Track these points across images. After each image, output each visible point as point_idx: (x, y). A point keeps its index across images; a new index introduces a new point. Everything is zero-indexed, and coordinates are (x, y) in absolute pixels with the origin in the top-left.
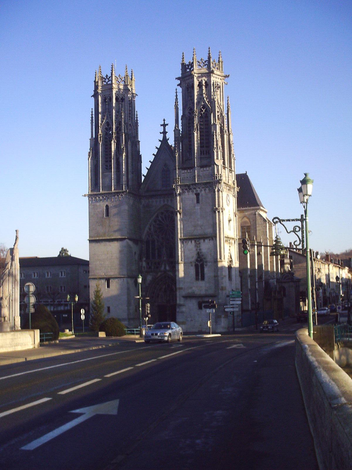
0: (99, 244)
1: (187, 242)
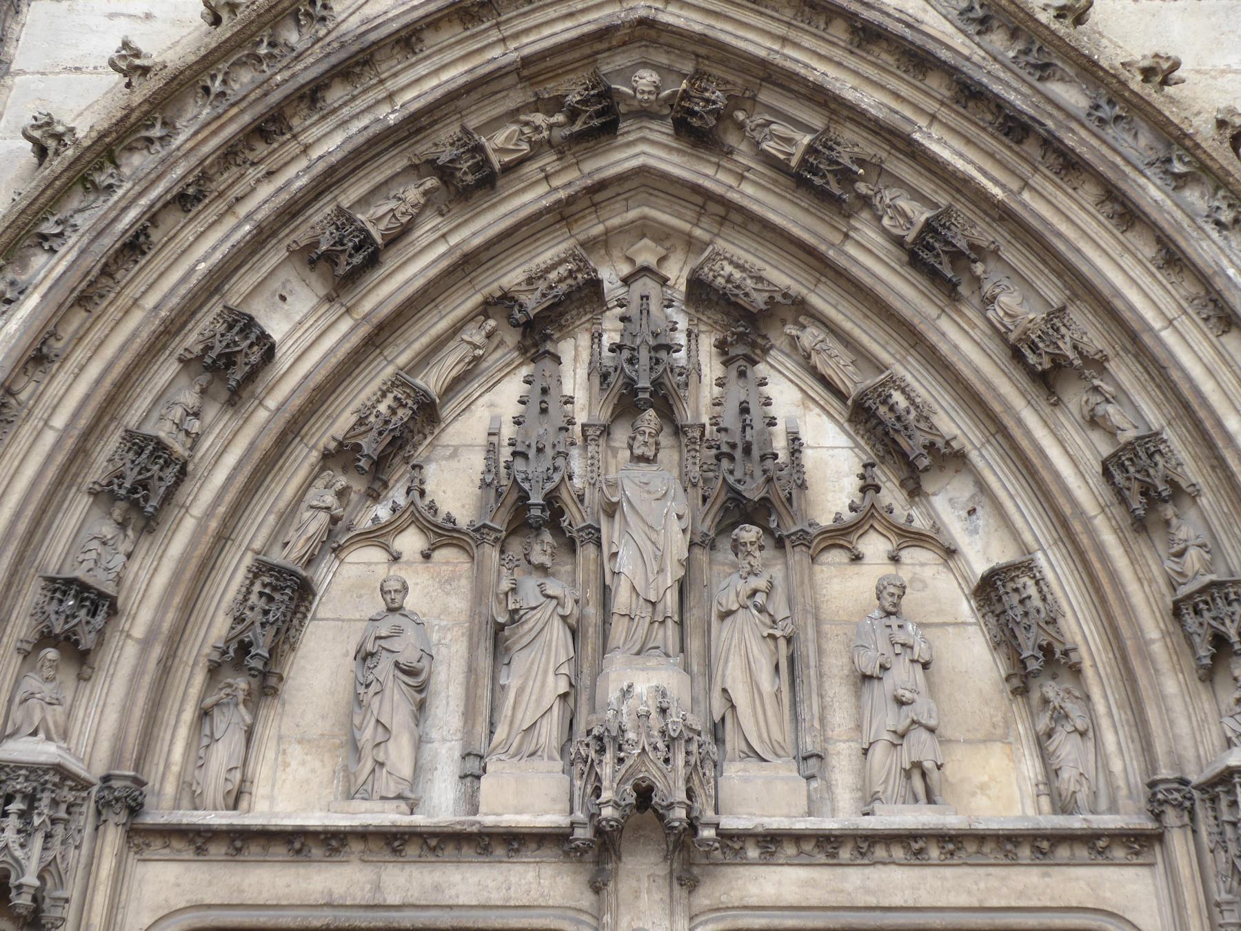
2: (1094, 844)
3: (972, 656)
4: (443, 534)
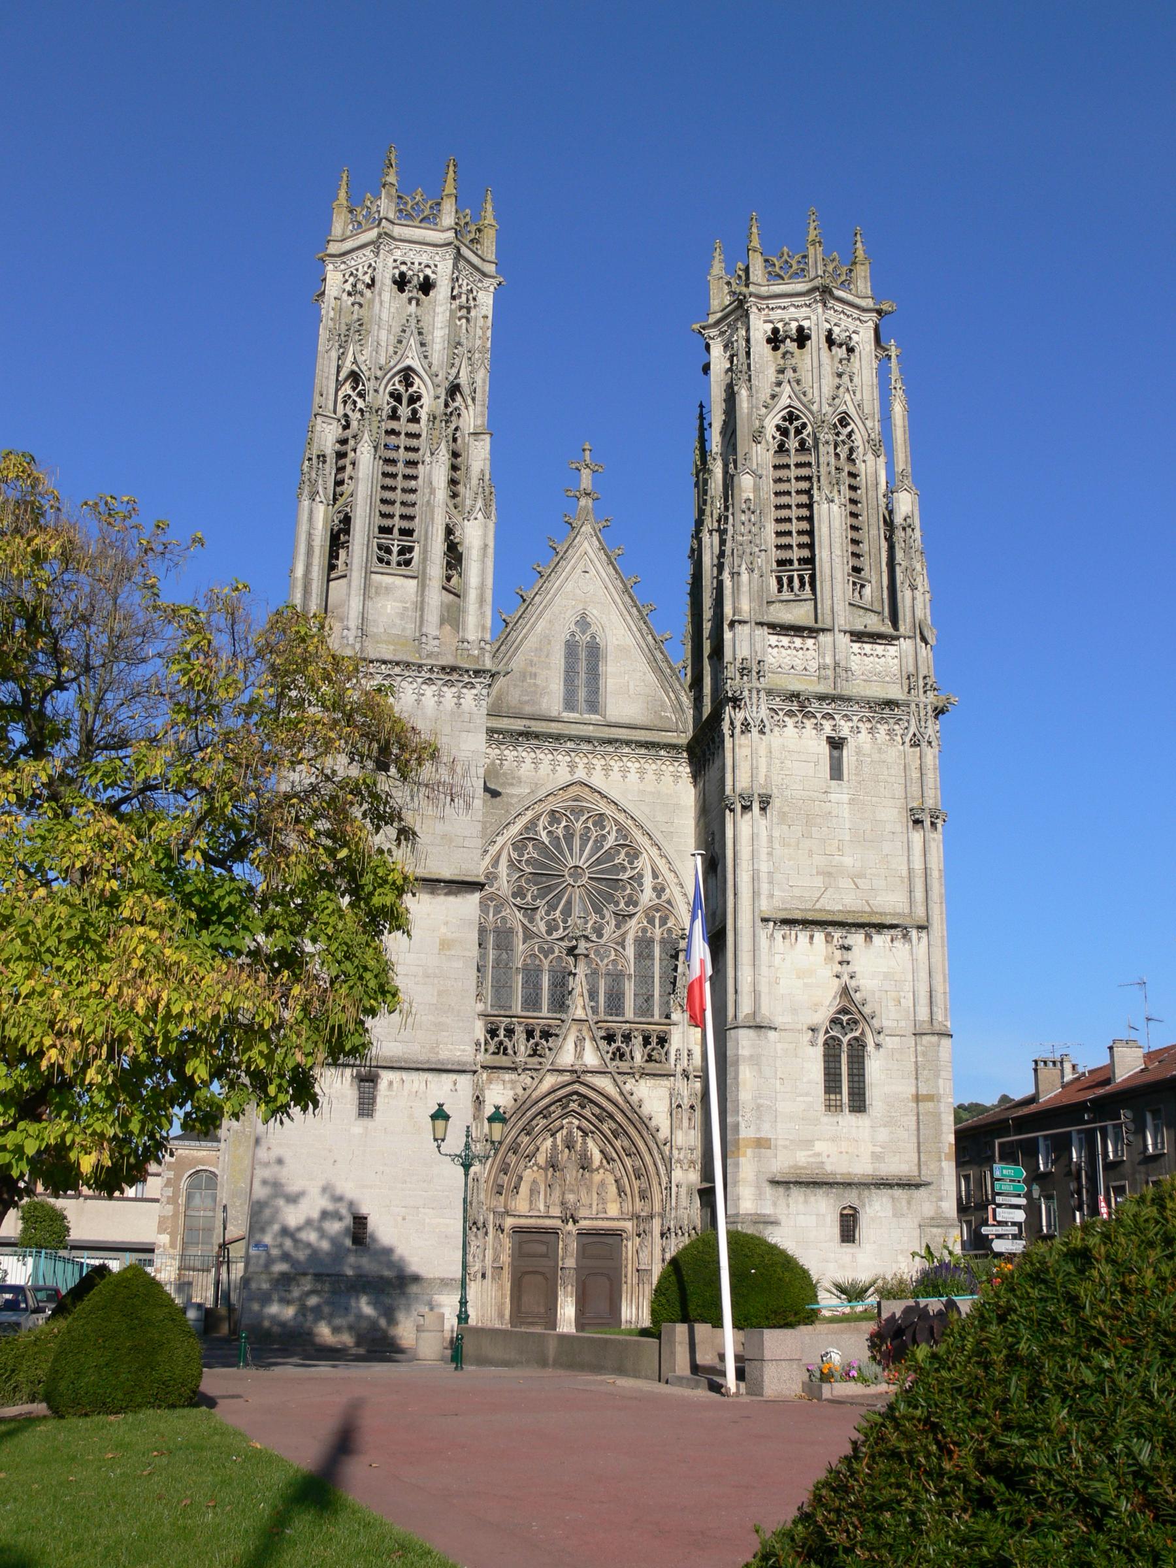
2: (624, 1219)
3: (613, 1189)
4: (540, 1168)
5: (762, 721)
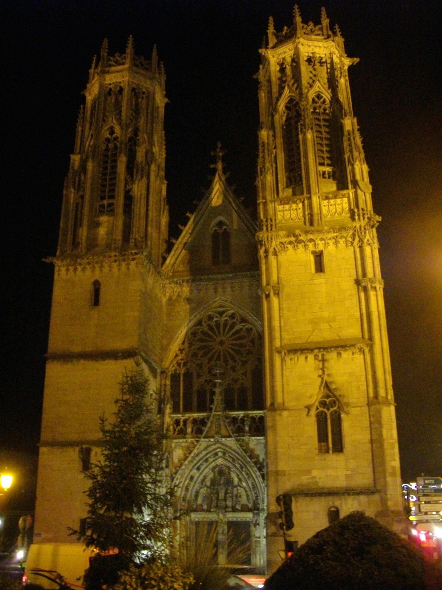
0: (69, 366)
1: (296, 358)
5: (274, 249)
